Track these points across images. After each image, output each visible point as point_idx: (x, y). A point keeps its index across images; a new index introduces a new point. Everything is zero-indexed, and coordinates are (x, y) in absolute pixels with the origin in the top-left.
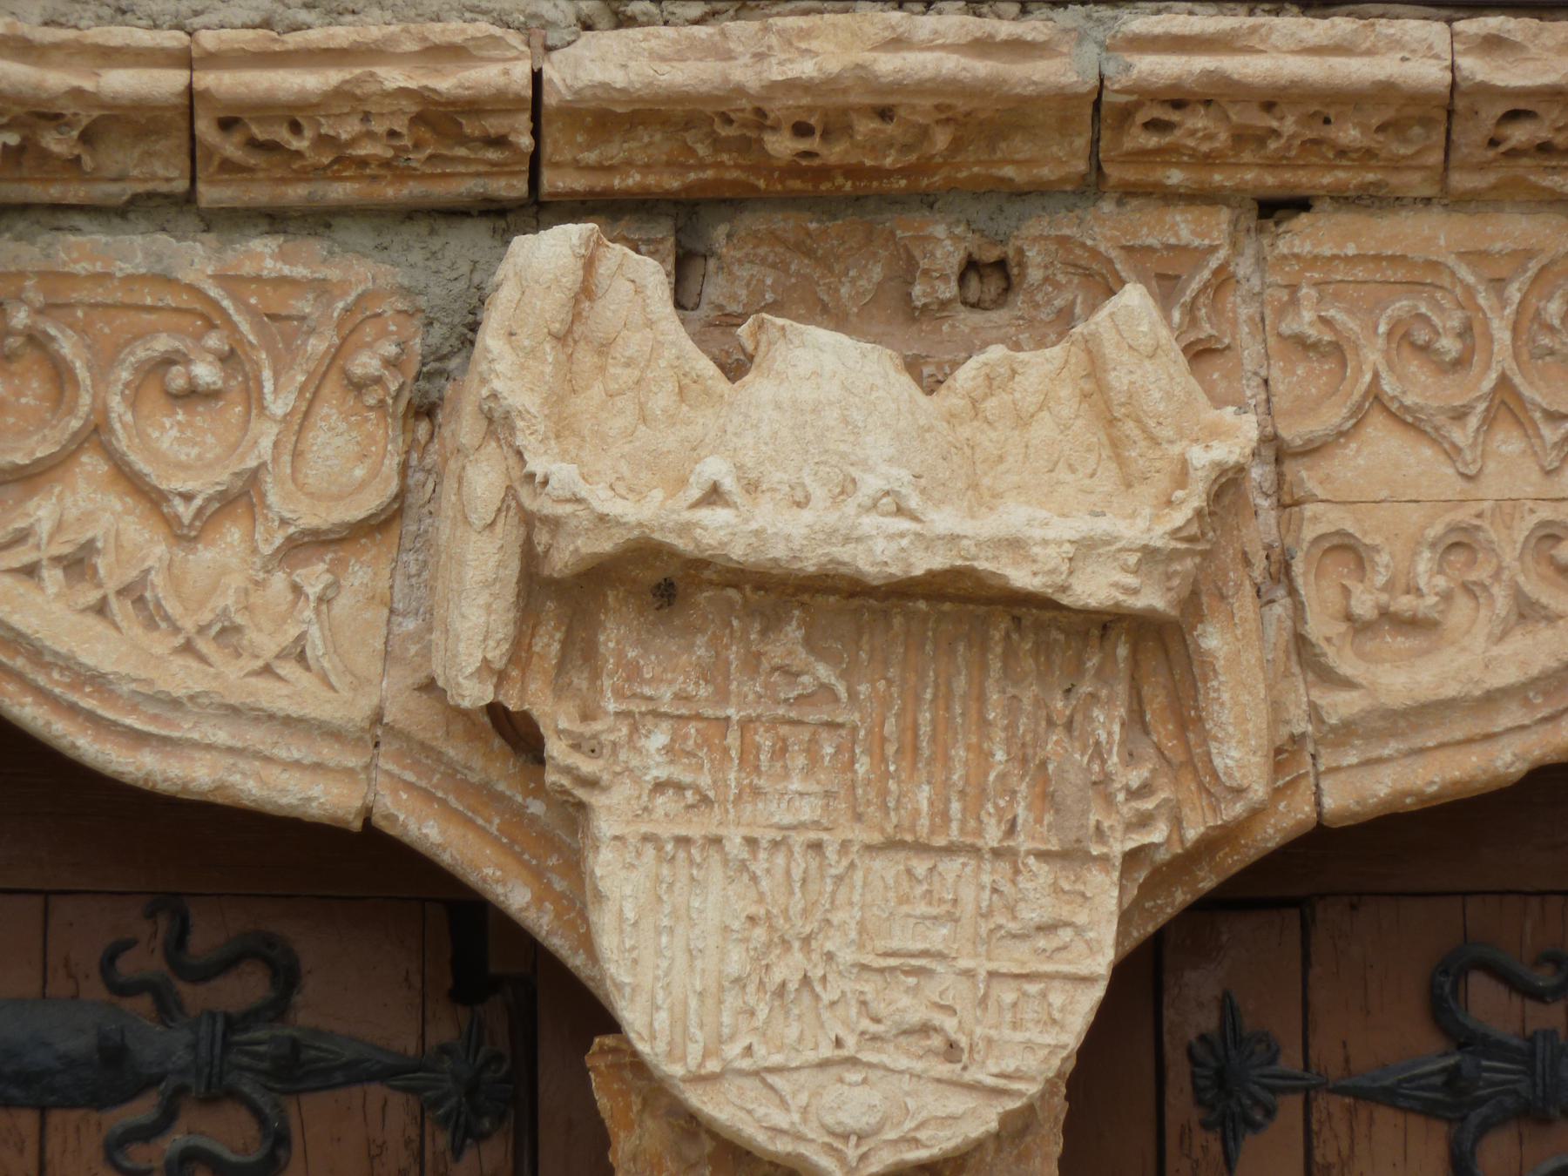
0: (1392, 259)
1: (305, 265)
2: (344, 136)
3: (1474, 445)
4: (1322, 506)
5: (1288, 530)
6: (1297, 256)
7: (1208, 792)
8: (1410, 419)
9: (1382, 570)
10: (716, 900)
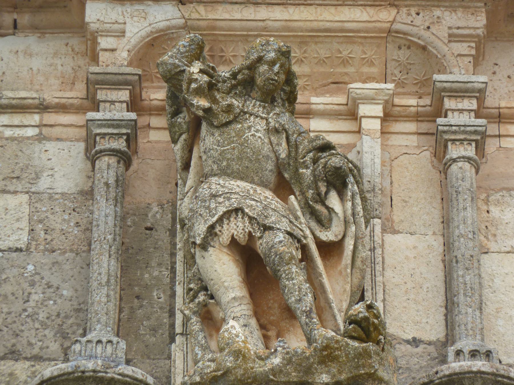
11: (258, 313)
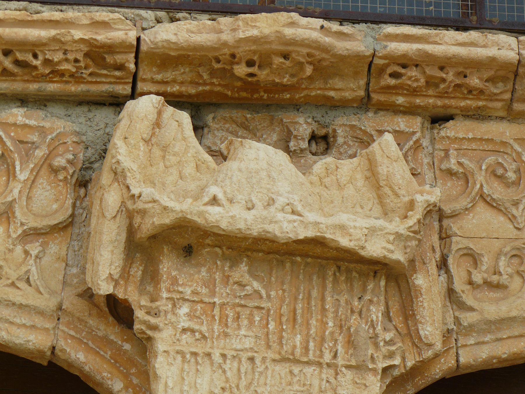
0: (487, 140)
1: (35, 120)
2: (56, 60)
3: (522, 216)
4: (459, 238)
5: (445, 247)
6: (448, 137)
7: (417, 346)
8: (495, 205)
9: (485, 264)
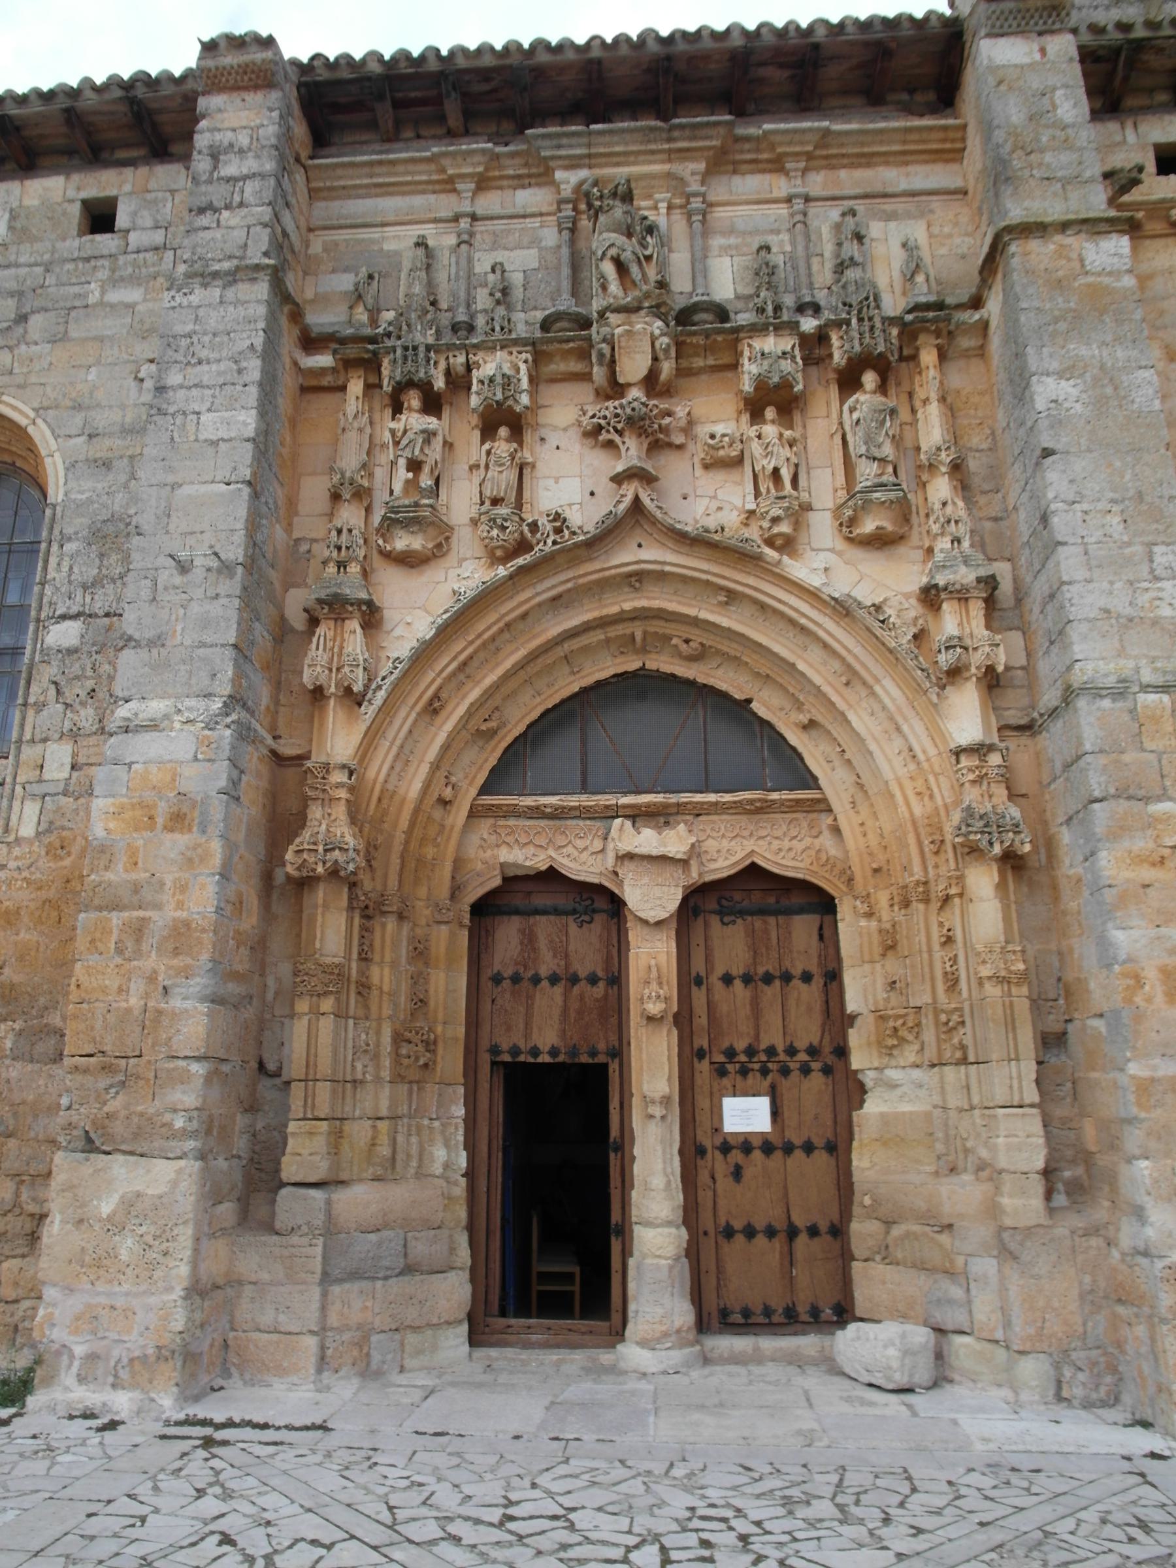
10: (638, 891)
11: (622, 284)
